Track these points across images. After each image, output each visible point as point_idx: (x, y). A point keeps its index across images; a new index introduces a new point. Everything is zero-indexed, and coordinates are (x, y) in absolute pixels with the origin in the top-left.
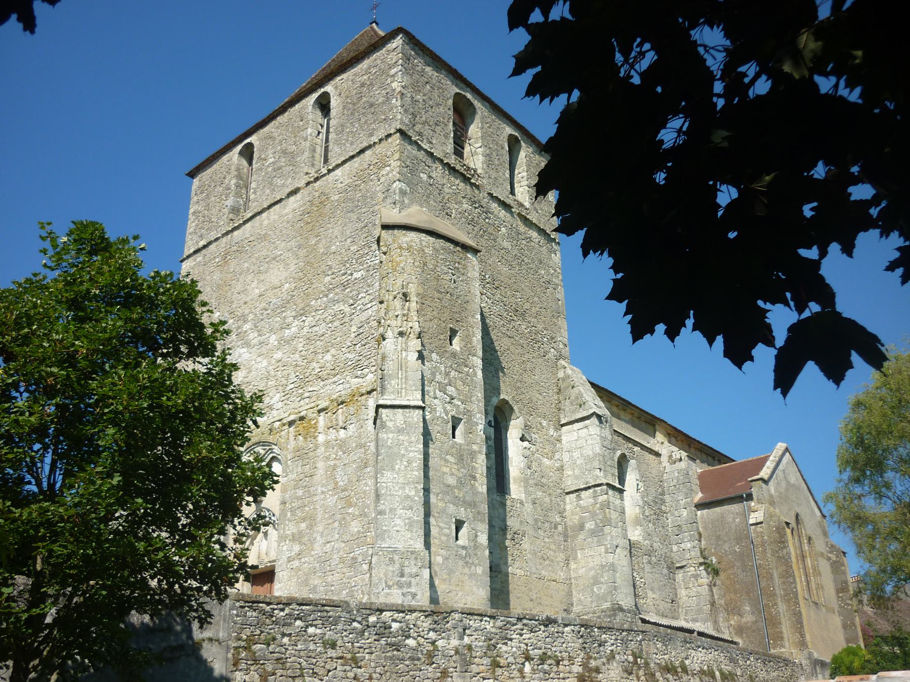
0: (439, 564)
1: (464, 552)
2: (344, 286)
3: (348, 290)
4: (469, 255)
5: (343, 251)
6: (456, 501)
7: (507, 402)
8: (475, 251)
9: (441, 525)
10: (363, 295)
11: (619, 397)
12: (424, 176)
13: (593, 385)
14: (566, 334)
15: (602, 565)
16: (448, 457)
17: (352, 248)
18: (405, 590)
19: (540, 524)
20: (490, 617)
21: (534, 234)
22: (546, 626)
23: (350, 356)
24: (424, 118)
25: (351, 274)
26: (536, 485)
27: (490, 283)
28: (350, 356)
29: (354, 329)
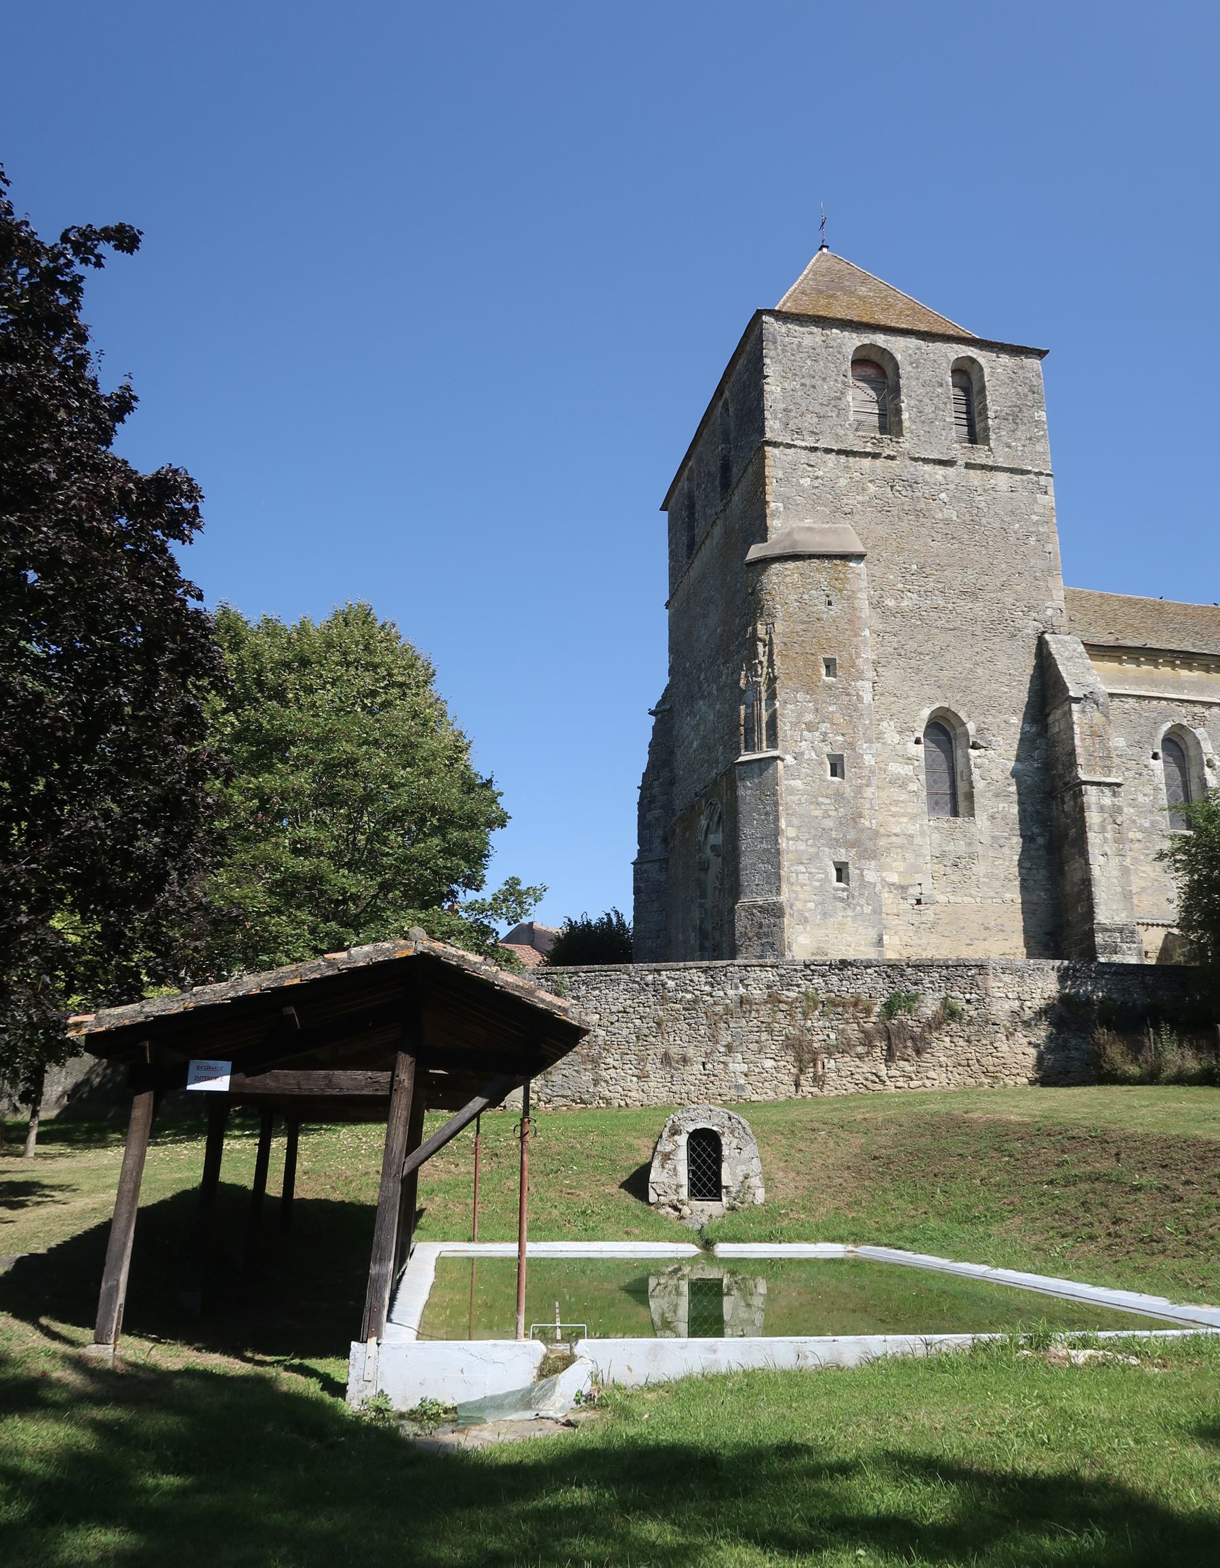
0: (810, 910)
4: (851, 564)
6: (835, 843)
7: (948, 710)
8: (860, 557)
9: (813, 870)
12: (806, 482)
16: (821, 799)
18: (764, 940)
20: (772, 967)
21: (1002, 480)
24: (803, 409)
26: (997, 795)
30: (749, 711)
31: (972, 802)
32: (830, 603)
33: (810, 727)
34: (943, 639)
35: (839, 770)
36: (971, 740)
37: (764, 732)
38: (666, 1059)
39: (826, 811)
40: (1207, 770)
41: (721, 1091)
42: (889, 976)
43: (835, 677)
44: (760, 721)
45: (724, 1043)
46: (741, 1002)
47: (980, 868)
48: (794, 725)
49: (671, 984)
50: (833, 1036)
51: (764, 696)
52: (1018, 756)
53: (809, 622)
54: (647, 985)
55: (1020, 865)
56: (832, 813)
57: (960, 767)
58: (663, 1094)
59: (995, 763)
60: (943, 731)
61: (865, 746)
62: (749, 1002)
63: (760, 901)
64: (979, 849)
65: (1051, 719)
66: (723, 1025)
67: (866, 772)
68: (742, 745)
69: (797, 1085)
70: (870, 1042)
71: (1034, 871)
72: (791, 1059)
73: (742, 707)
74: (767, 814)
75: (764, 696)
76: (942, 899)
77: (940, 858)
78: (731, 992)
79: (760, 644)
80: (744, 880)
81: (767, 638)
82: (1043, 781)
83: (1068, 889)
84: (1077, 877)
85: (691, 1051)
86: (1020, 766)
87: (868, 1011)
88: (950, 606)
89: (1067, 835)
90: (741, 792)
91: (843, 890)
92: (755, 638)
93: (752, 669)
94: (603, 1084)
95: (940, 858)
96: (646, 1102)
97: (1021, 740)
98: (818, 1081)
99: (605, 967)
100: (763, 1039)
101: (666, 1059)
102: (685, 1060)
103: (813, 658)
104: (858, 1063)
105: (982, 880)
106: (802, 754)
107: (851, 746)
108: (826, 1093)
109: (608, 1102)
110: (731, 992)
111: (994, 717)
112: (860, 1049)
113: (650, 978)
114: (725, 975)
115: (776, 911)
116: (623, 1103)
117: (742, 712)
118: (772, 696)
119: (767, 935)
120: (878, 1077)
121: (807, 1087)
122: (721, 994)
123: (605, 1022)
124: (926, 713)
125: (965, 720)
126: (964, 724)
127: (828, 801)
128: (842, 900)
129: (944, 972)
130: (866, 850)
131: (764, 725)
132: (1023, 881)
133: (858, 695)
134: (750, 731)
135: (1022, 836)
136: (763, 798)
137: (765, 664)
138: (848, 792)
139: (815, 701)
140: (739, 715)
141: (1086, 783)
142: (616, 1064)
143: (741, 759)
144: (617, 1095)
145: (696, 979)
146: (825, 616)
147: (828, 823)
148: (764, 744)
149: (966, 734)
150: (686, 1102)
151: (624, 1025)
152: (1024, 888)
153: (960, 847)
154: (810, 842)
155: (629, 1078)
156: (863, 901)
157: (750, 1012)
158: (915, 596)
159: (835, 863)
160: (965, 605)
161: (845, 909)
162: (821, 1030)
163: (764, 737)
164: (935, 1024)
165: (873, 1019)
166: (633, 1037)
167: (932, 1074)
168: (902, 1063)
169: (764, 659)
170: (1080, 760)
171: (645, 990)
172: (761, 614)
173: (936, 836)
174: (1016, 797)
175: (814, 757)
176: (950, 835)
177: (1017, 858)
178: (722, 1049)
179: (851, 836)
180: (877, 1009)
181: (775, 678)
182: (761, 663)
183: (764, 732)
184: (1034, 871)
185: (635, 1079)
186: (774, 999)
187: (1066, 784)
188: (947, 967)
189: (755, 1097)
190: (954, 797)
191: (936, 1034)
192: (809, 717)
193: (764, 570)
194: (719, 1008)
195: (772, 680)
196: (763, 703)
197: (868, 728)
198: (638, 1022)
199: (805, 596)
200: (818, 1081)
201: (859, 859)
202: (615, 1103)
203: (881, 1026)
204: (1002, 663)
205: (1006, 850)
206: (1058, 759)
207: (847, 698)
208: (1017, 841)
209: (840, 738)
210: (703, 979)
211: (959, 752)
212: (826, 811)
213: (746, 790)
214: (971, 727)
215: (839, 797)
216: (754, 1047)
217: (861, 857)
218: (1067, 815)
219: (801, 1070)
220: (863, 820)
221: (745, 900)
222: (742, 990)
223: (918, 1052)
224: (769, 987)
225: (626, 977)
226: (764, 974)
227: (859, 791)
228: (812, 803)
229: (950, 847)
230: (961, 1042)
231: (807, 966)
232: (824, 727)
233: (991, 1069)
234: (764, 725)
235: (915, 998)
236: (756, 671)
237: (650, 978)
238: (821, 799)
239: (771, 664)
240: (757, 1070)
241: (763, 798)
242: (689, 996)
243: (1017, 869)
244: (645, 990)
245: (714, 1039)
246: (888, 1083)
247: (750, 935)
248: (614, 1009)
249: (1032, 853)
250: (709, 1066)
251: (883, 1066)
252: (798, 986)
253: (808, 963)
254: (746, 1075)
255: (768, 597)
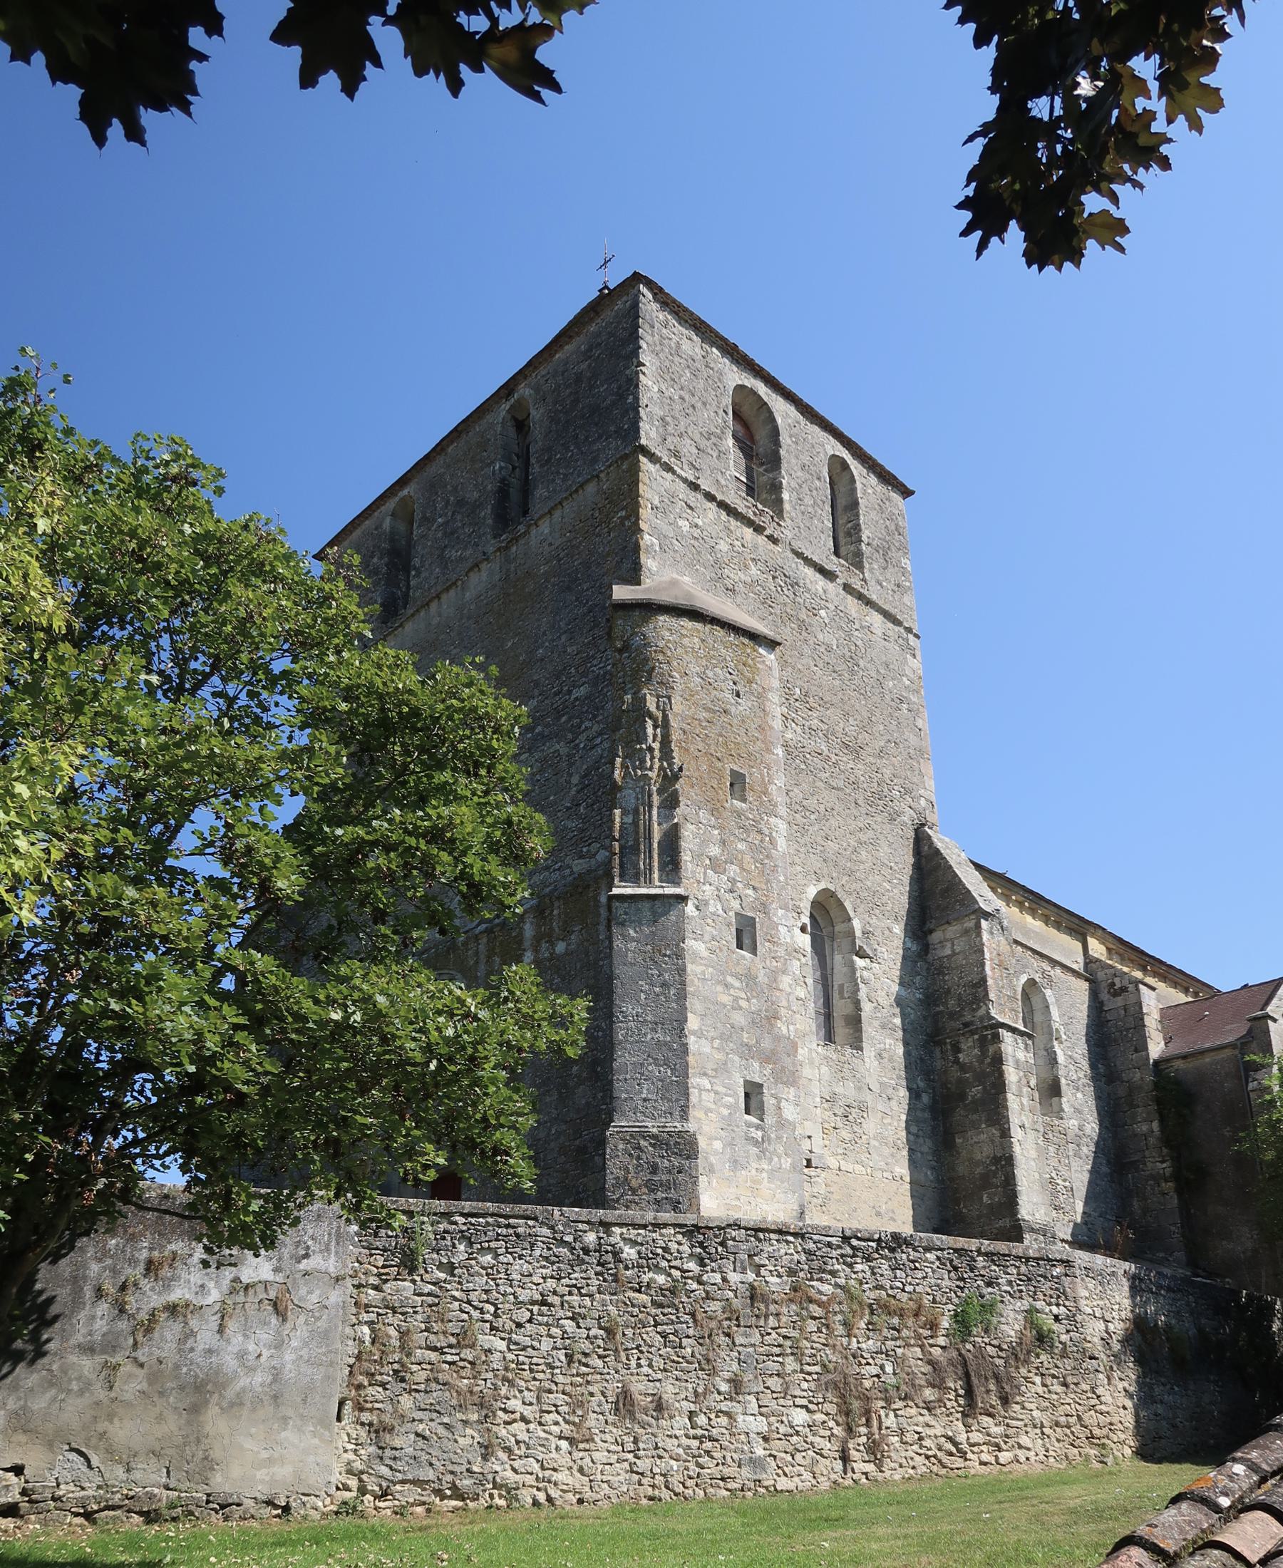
0: (716, 1153)
1: (760, 1133)
2: (558, 713)
3: (564, 719)
5: (556, 655)
6: (748, 1052)
9: (721, 1089)
10: (587, 724)
11: (1023, 887)
13: (978, 867)
14: (931, 784)
15: (995, 1157)
16: (729, 979)
17: (569, 650)
18: (660, 1195)
19: (890, 1091)
22: (892, 1250)
23: (570, 824)
25: (569, 692)
26: (883, 1027)
27: (800, 700)
28: (570, 824)
29: (575, 780)
30: (629, 819)
31: (860, 1030)
32: (738, 695)
33: (715, 865)
34: (829, 798)
35: (746, 941)
36: (858, 942)
37: (656, 857)
38: (624, 1404)
39: (736, 999)
40: (1055, 1043)
41: (727, 1471)
42: (956, 1269)
43: (744, 801)
44: (649, 838)
45: (727, 1375)
46: (752, 1297)
47: (871, 1125)
48: (697, 856)
49: (629, 1253)
50: (889, 1369)
51: (656, 800)
52: (901, 978)
53: (714, 712)
54: (586, 1251)
55: (907, 1128)
56: (743, 1004)
57: (839, 978)
58: (619, 1475)
59: (880, 978)
60: (827, 920)
61: (780, 912)
62: (765, 1299)
63: (652, 1127)
64: (869, 1098)
65: (936, 937)
66: (722, 1340)
67: (781, 952)
68: (616, 871)
69: (845, 1458)
70: (943, 1380)
71: (921, 1140)
72: (832, 1409)
73: (617, 812)
74: (664, 984)
75: (656, 800)
76: (833, 1162)
77: (830, 1100)
78: (734, 1277)
79: (649, 723)
80: (621, 1090)
81: (660, 715)
82: (925, 1018)
83: (962, 1170)
84: (983, 1152)
85: (670, 1389)
86: (903, 993)
87: (933, 1326)
88: (834, 758)
89: (962, 1096)
90: (618, 944)
91: (758, 1127)
92: (640, 712)
93: (635, 757)
94: (503, 1455)
95: (830, 1100)
96: (588, 1495)
97: (904, 958)
98: (875, 1451)
99: (507, 1209)
100: (789, 1369)
101: (624, 1404)
102: (660, 1407)
103: (719, 765)
104: (928, 1418)
105: (873, 1142)
106: (706, 903)
107: (764, 909)
108: (888, 1474)
109: (510, 1492)
110: (734, 1277)
111: (878, 918)
112: (929, 1394)
113: (591, 1238)
114: (722, 1244)
115: (685, 1147)
116: (541, 1497)
117: (618, 820)
118: (671, 802)
119: (667, 1186)
120: (955, 1444)
121: (861, 1465)
122: (717, 1278)
123: (504, 1322)
124: (812, 892)
125: (852, 914)
126: (850, 919)
127: (737, 984)
128: (756, 1143)
129: (1023, 1269)
130: (783, 1069)
131: (655, 845)
132: (911, 1151)
133: (770, 836)
134: (631, 850)
135: (909, 1089)
136: (658, 958)
137: (657, 753)
138: (762, 978)
139: (722, 828)
140: (613, 821)
141: (1003, 1026)
142: (528, 1412)
143: (615, 891)
144: (530, 1480)
145: (673, 1246)
146: (733, 710)
147: (739, 1019)
148: (656, 876)
149: (851, 934)
150: (665, 1494)
151: (543, 1330)
152: (913, 1163)
153: (846, 1090)
154: (717, 1043)
155: (554, 1442)
156: (780, 1150)
157: (766, 1317)
158: (799, 729)
159: (746, 1082)
160: (847, 762)
161: (759, 1158)
162: (875, 1357)
163: (656, 864)
164: (1018, 1355)
165: (942, 1341)
166: (561, 1355)
167: (1024, 1440)
168: (986, 1420)
169: (656, 746)
170: (992, 996)
171: (583, 1262)
172: (649, 678)
173: (824, 1069)
174: (900, 1034)
175: (721, 912)
176: (840, 1071)
177: (904, 1117)
178: (724, 1387)
179: (767, 1044)
180: (945, 1323)
181: (676, 777)
182: (650, 749)
183: (656, 857)
184: (921, 1140)
185: (564, 1444)
186: (798, 1294)
187: (966, 1025)
188: (1028, 1259)
189: (783, 1483)
190: (839, 1021)
191: (1023, 1371)
192: (714, 850)
193: (646, 621)
194: (715, 1306)
195: (670, 778)
196: (655, 812)
197: (783, 888)
198: (569, 1325)
199: (710, 674)
200: (875, 1451)
201: (776, 1083)
202: (526, 1496)
203: (955, 1354)
204: (884, 851)
205: (894, 1103)
206: (948, 991)
207: (759, 837)
208: (903, 1093)
209: (750, 892)
210: (686, 1248)
211: (838, 958)
212: (736, 999)
213: (628, 944)
214: (857, 924)
215: (749, 979)
216: (774, 1383)
217: (778, 1080)
218: (963, 1068)
219: (849, 1430)
220: (779, 1024)
221: (621, 1122)
222: (751, 1276)
223: (1005, 1401)
224: (792, 1273)
225: (545, 1231)
226: (783, 1249)
227: (774, 976)
228: (719, 982)
229: (839, 1089)
230: (1059, 1389)
231: (846, 1239)
232: (733, 870)
233: (1097, 1432)
234: (655, 845)
235: (988, 1308)
236: (643, 761)
237: (591, 1238)
238: (729, 979)
239: (666, 753)
240: (783, 1429)
241: (658, 958)
242: (661, 1279)
243: (904, 1133)
244: (583, 1262)
245: (708, 1366)
246: (970, 1455)
247: (634, 1183)
248: (524, 1295)
249: (919, 1114)
250: (701, 1420)
251: (960, 1424)
252: (833, 1273)
253: (848, 1233)
254: (766, 1439)
255: (661, 657)
